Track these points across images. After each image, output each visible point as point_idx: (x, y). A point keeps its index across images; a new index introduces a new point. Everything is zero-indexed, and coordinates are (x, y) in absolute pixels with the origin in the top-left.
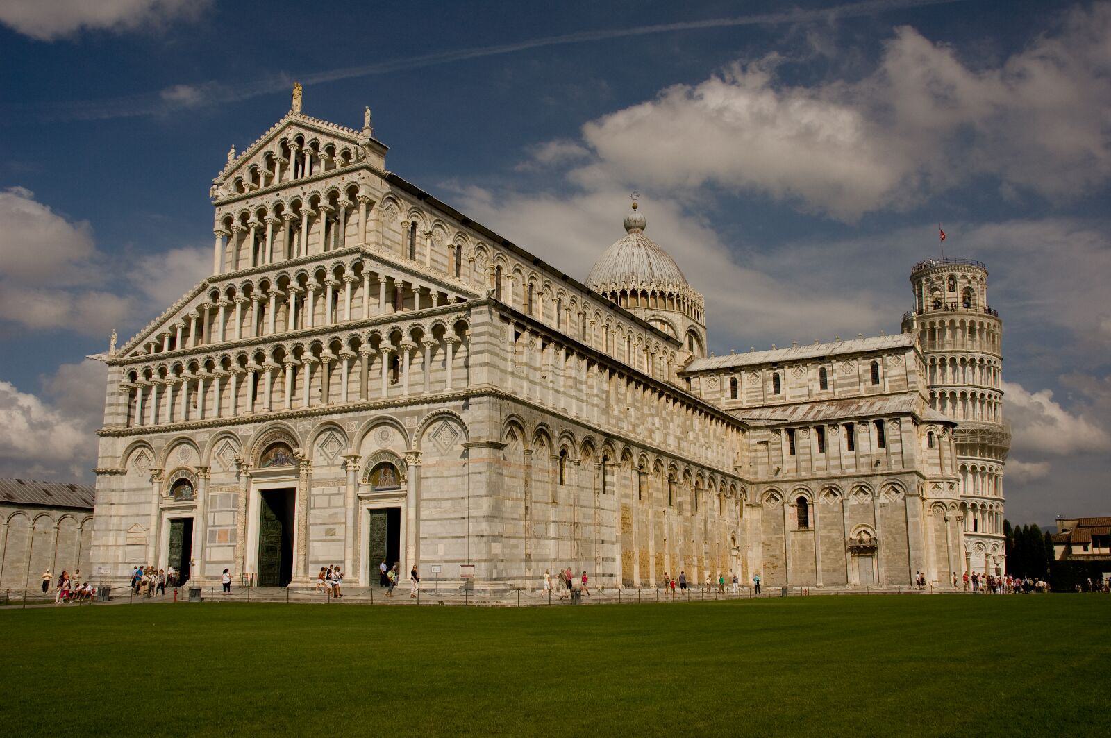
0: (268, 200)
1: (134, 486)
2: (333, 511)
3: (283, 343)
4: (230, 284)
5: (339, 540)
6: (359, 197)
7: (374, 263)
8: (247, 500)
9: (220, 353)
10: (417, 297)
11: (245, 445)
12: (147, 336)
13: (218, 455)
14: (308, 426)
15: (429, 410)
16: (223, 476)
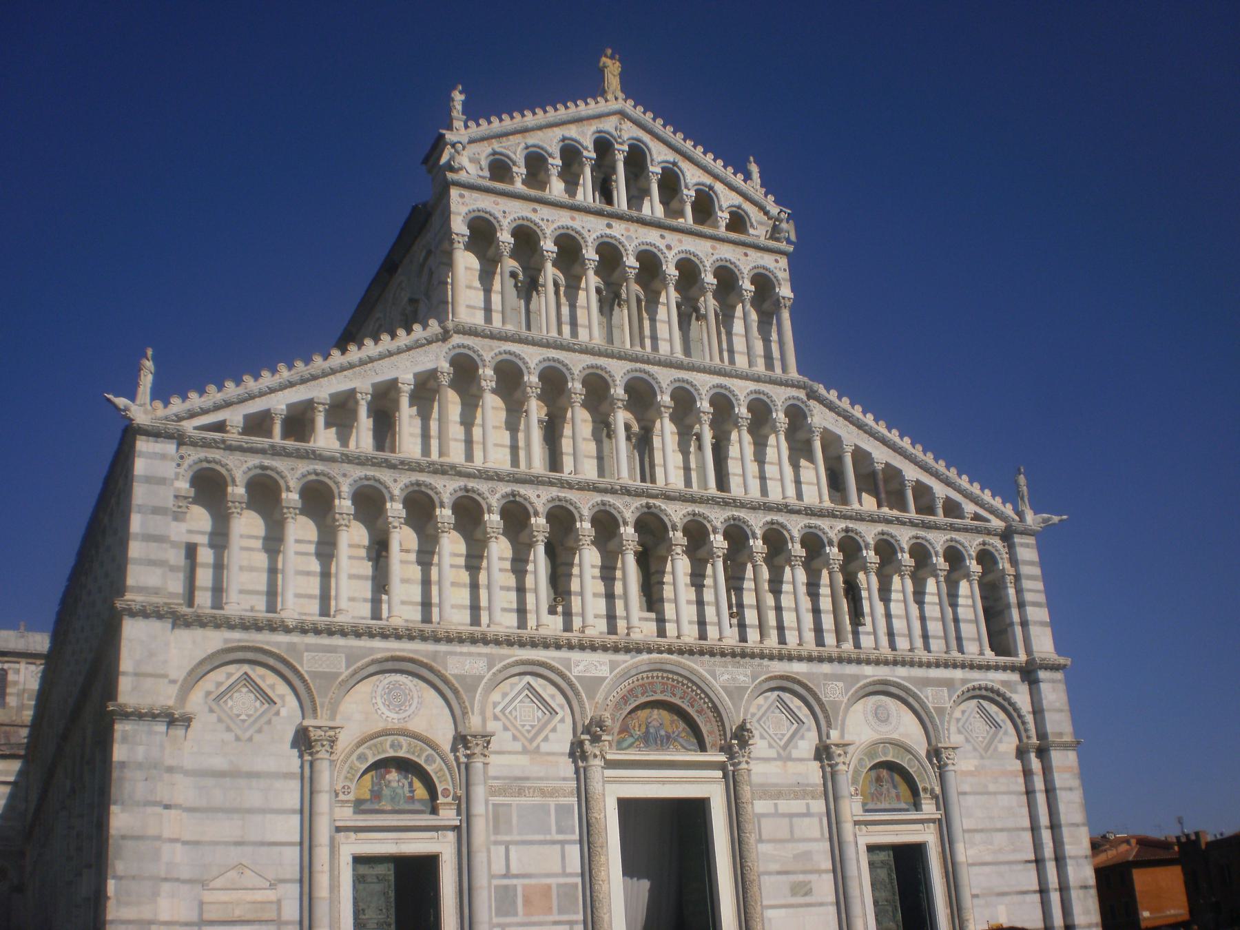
0: (588, 226)
1: (219, 763)
2: (803, 847)
3: (663, 507)
4: (510, 353)
5: (821, 904)
6: (784, 298)
7: (831, 415)
8: (605, 817)
9: (505, 489)
10: (909, 494)
11: (591, 697)
12: (262, 394)
13: (503, 711)
14: (742, 678)
15: (964, 681)
16: (523, 760)
